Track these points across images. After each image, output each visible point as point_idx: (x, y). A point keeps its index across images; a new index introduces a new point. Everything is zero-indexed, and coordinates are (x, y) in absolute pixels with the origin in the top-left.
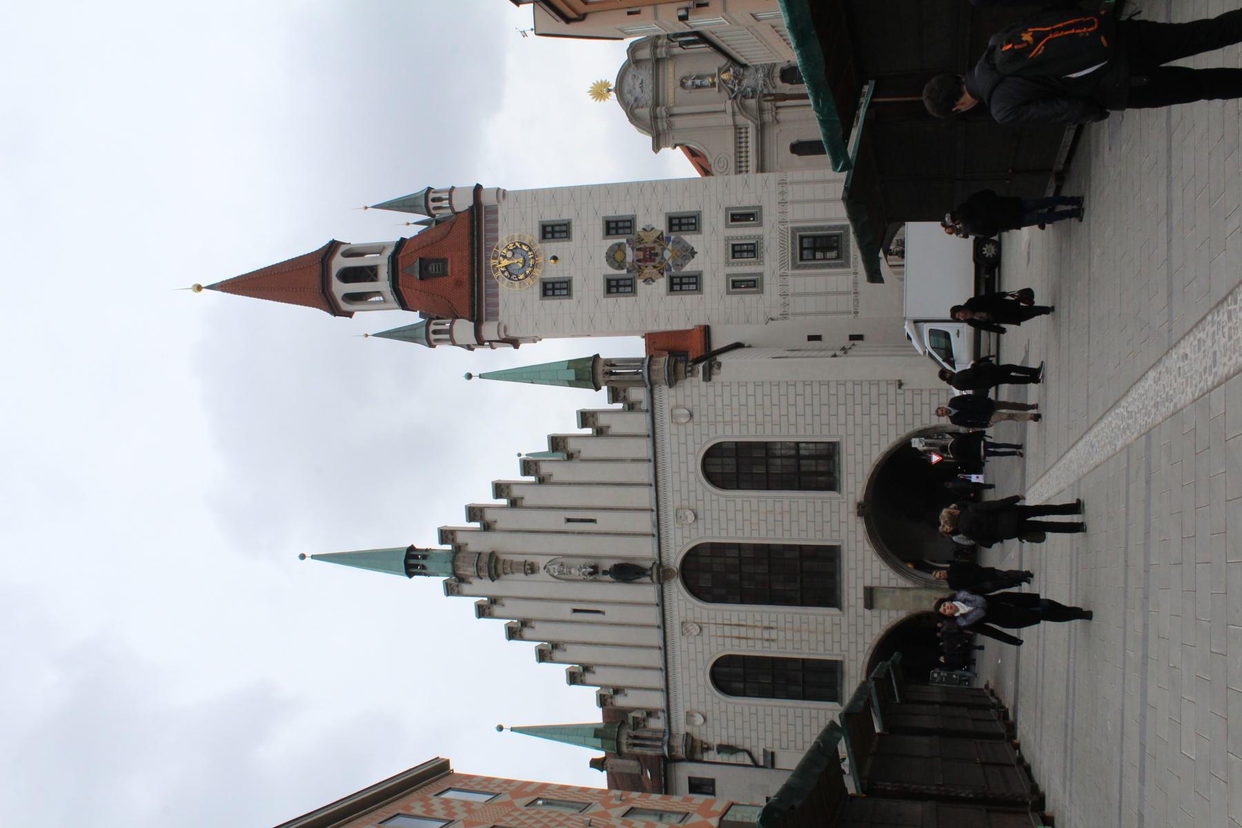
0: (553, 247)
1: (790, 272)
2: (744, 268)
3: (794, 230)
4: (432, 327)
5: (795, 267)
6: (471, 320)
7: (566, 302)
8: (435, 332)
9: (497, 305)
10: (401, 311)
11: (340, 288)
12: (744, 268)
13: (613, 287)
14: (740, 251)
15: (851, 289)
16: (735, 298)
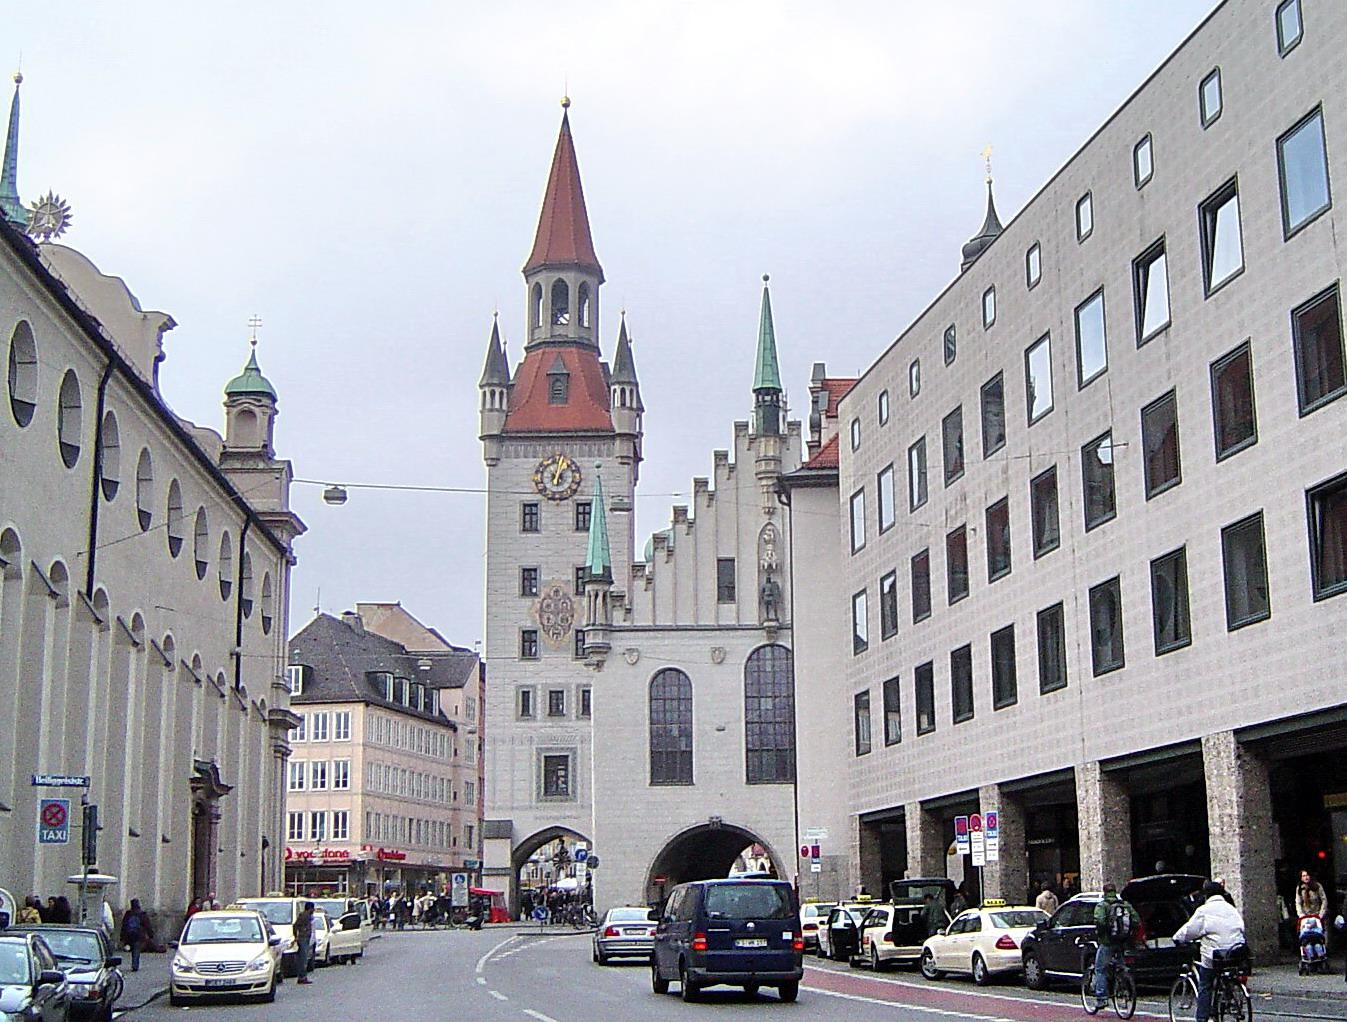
0: (568, 511)
1: (534, 748)
2: (540, 703)
3: (574, 750)
4: (498, 390)
5: (539, 751)
6: (503, 431)
7: (518, 526)
8: (493, 394)
9: (517, 457)
10: (526, 344)
11: (546, 280)
12: (540, 703)
13: (529, 576)
14: (556, 699)
15: (515, 805)
16: (513, 693)
